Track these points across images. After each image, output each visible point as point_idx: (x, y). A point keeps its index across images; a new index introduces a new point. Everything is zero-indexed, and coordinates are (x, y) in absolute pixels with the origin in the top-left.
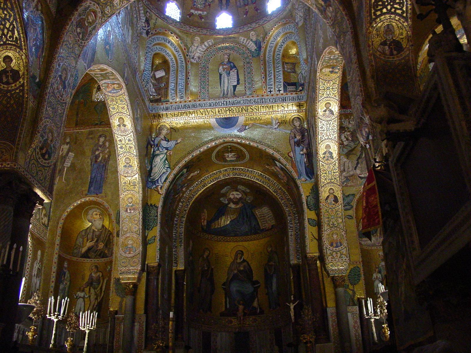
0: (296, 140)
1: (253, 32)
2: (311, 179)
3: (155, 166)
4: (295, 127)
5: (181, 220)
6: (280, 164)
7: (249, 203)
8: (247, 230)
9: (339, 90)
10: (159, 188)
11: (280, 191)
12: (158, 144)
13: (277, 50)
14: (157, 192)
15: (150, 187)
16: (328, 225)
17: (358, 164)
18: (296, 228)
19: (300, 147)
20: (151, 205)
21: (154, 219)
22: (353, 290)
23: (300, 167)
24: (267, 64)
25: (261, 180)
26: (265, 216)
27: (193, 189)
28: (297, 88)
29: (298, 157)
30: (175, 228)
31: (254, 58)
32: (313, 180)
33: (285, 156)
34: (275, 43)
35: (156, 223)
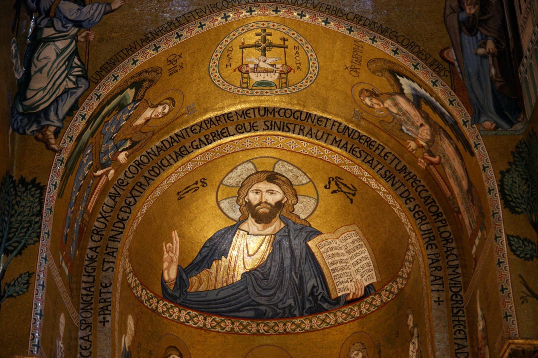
0: (463, 16)
2: (511, 124)
3: (40, 71)
5: (107, 247)
6: (416, 86)
7: (305, 220)
8: (291, 301)
10: (48, 133)
11: (403, 175)
12: (49, 10)
14: (44, 145)
15: (21, 131)
18: (451, 279)
19: (475, 34)
20: (22, 181)
21: (29, 222)
25: (347, 143)
26: (346, 261)
27: (146, 161)
30: (89, 269)
32: (519, 126)
33: (430, 61)
35: (34, 235)
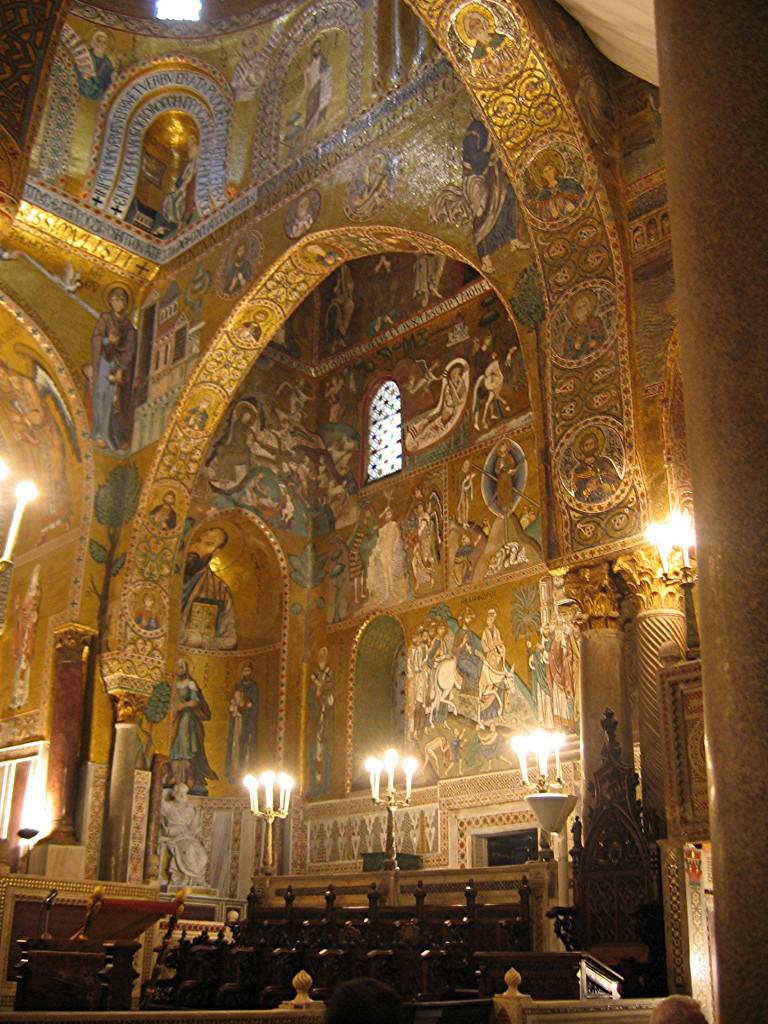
0: (106, 341)
1: (101, 33)
2: (116, 448)
4: (112, 312)
9: (302, 300)
13: (140, 111)
16: (141, 571)
17: (214, 454)
22: (148, 735)
23: (101, 412)
24: (109, 132)
28: (153, 227)
29: (102, 386)
31: (82, 98)
32: (121, 452)
34: (145, 93)
